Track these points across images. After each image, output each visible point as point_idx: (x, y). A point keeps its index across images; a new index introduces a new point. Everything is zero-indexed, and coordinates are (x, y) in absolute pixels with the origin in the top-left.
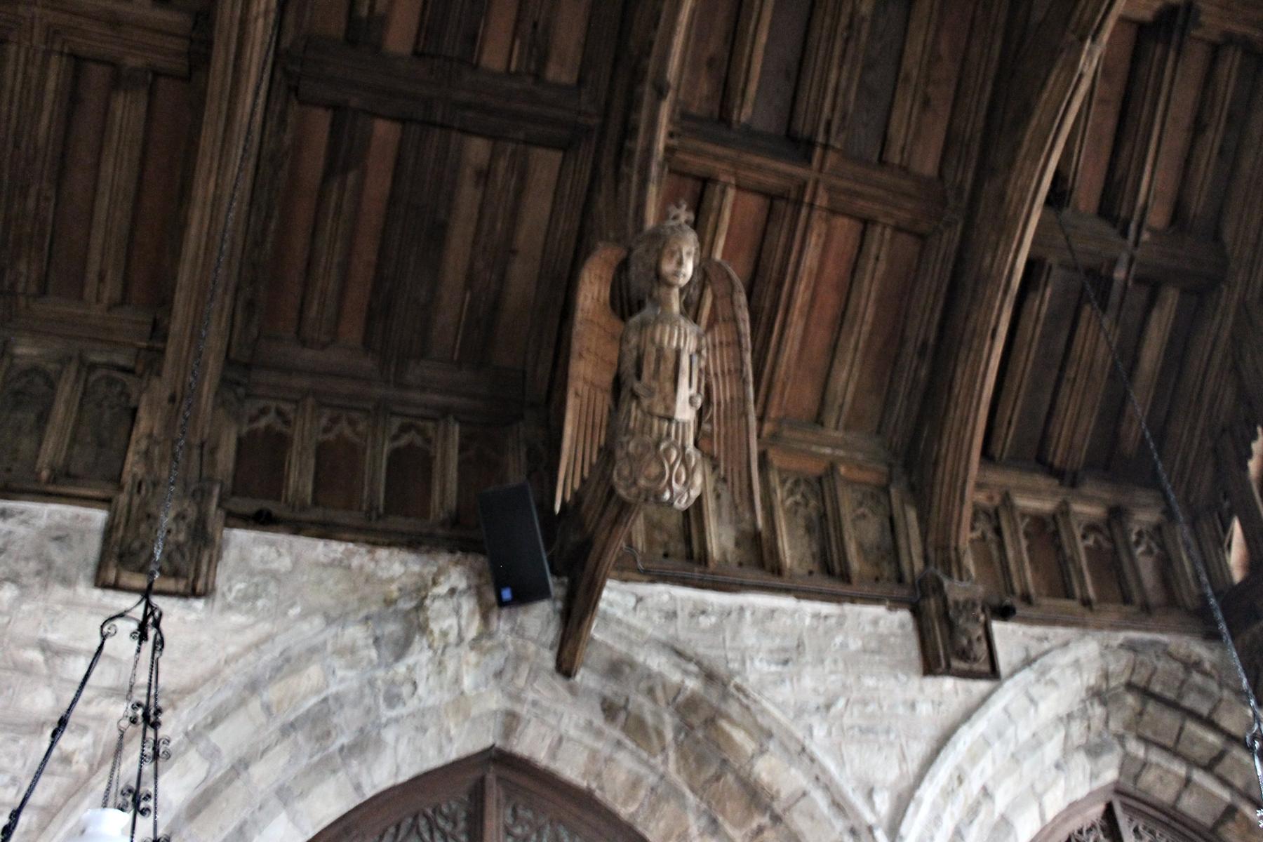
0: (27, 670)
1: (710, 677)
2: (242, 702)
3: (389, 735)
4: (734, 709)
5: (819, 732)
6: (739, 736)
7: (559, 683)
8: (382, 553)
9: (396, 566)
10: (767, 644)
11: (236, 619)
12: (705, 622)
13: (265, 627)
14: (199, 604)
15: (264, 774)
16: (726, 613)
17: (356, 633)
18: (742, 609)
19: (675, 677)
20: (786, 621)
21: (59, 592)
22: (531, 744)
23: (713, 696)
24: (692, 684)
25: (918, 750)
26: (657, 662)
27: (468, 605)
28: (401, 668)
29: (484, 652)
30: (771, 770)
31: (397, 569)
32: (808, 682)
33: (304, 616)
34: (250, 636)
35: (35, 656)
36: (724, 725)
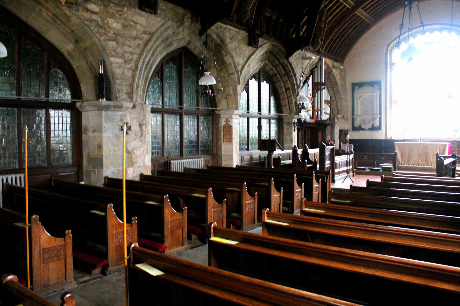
0: (131, 26)
1: (222, 41)
2: (160, 37)
3: (174, 43)
4: (224, 47)
5: (234, 53)
6: (223, 52)
7: (198, 37)
8: (179, 7)
9: (180, 11)
10: (230, 36)
11: (159, 19)
12: (222, 30)
13: (163, 21)
14: (153, 15)
15: (159, 49)
16: (224, 29)
17: (175, 24)
18: (226, 28)
19: (217, 40)
20: (232, 31)
21: (134, 10)
22: (191, 47)
23: (221, 44)
24: (219, 41)
25: (246, 59)
26: (214, 36)
27: (190, 21)
28: (178, 31)
29: (189, 29)
30: (227, 59)
31: (180, 11)
32: (234, 44)
33: (168, 20)
34: (161, 23)
35: (132, 23)
36: (222, 50)
